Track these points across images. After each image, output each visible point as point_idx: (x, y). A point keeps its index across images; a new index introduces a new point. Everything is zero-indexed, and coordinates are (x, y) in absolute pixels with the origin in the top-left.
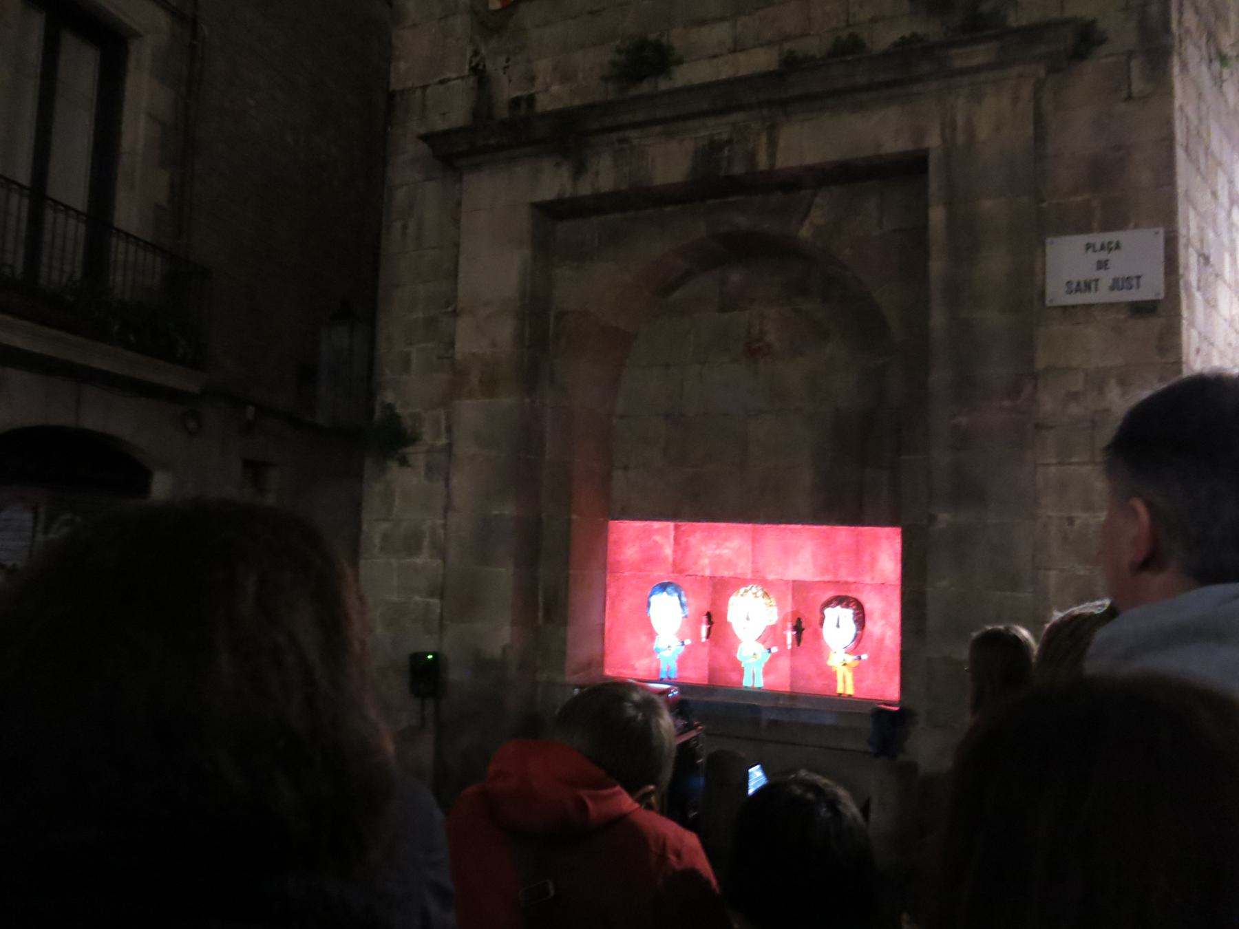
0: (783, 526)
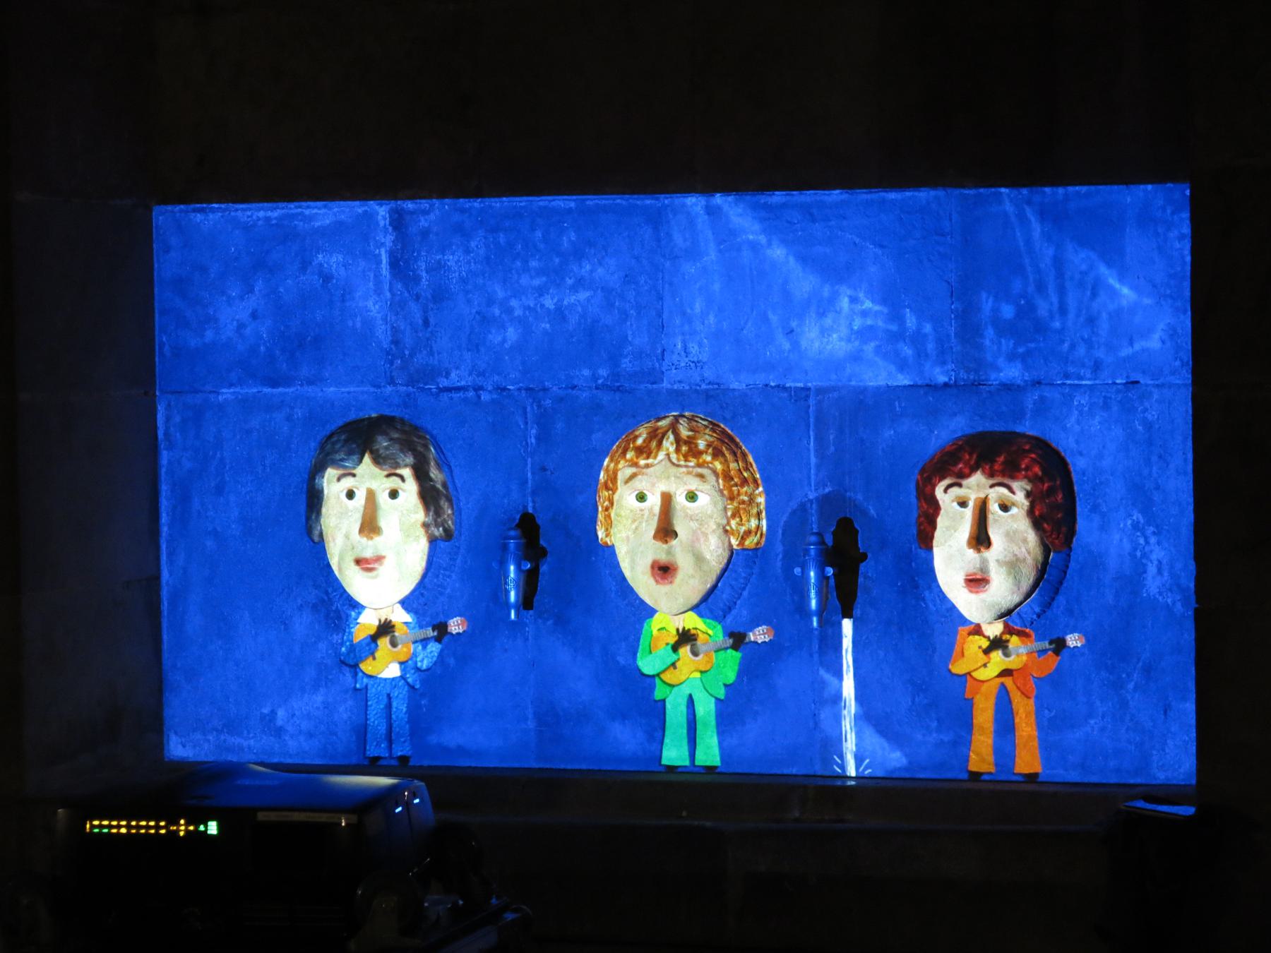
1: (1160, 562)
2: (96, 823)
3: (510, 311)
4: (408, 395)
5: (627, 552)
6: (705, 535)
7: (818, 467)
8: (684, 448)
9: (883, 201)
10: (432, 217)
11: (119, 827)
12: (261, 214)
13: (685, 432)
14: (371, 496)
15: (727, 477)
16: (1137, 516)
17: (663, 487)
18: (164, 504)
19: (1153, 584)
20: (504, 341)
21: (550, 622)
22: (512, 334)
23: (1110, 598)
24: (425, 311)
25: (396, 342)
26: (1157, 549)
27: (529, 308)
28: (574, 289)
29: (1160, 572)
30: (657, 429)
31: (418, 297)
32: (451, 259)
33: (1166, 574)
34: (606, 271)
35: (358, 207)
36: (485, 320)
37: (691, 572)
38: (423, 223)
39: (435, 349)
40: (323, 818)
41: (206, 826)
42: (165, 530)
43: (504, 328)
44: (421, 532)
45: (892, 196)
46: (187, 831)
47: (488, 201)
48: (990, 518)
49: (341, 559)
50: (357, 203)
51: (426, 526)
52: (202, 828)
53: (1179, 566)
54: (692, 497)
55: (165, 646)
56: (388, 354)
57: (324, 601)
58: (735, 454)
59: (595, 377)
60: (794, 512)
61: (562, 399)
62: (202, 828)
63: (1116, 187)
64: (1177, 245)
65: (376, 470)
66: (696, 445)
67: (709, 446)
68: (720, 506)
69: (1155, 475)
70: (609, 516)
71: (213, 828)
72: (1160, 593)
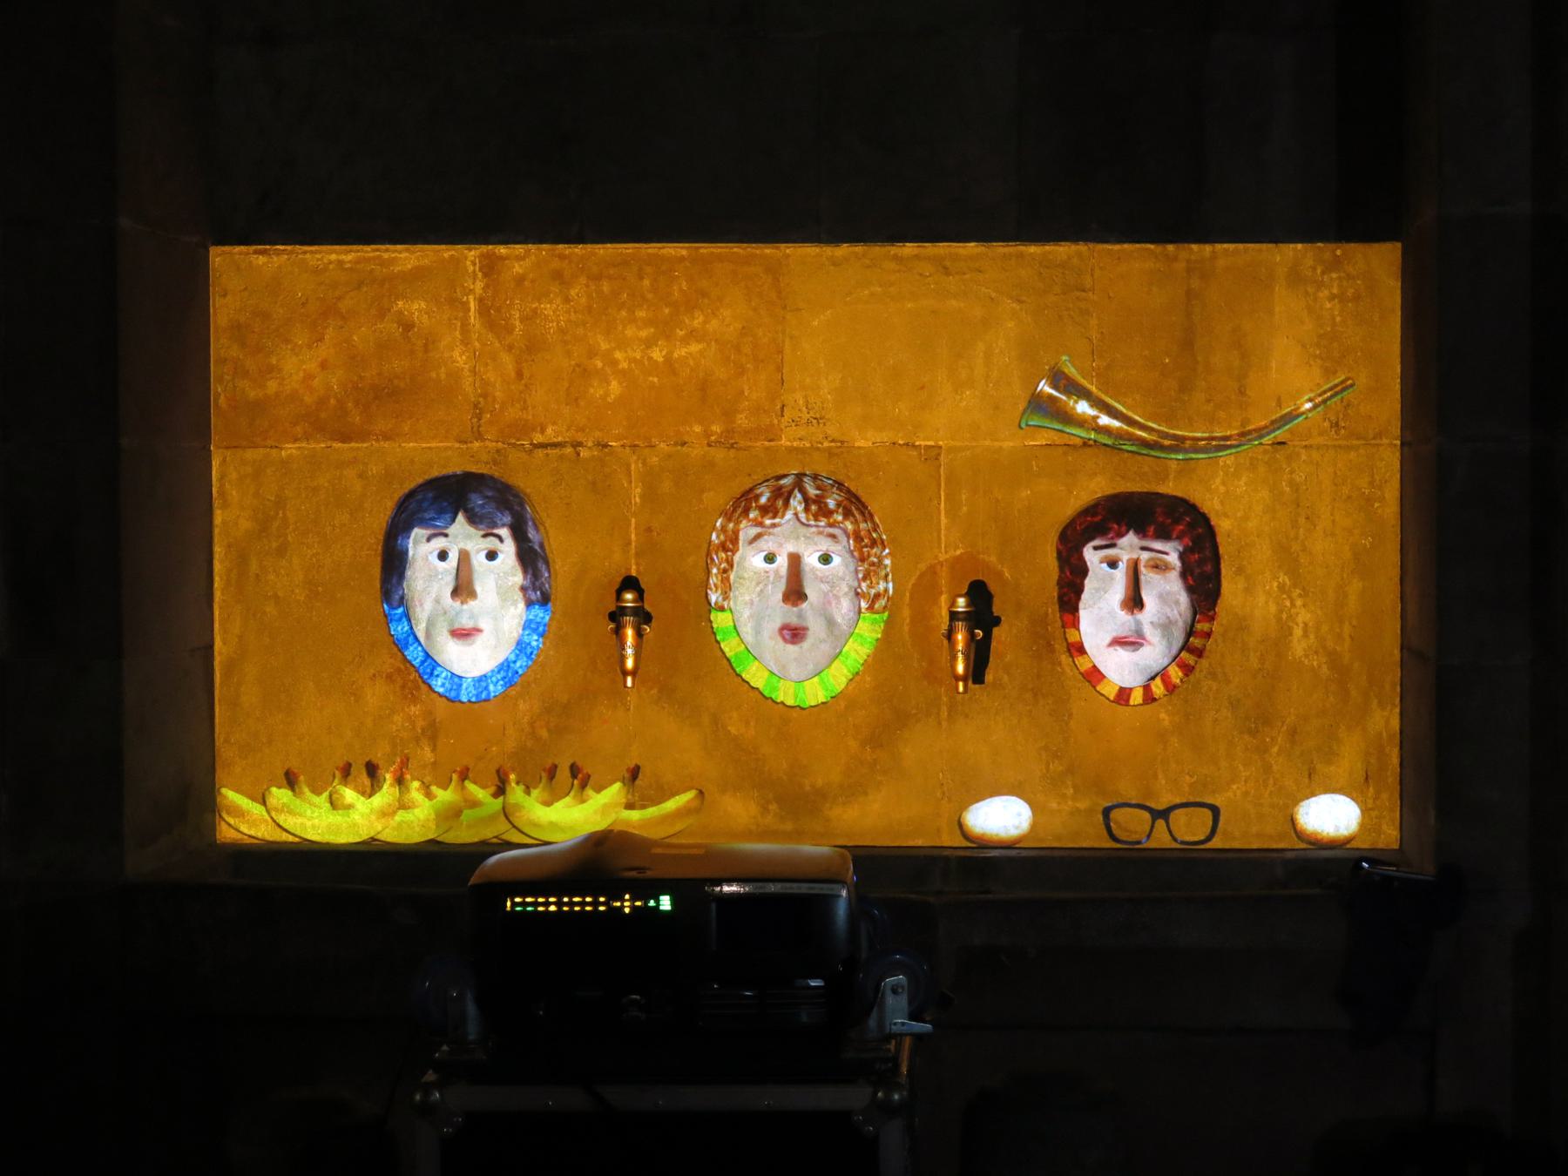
0: (909, 249)
1: (1306, 624)
2: (518, 900)
3: (614, 363)
4: (498, 451)
5: (751, 616)
6: (837, 597)
7: (947, 529)
8: (813, 507)
9: (1021, 256)
10: (527, 263)
11: (547, 904)
12: (333, 257)
13: (812, 492)
14: (464, 557)
15: (858, 537)
16: (1284, 578)
17: (791, 547)
18: (218, 567)
19: (1299, 646)
20: (607, 394)
21: (655, 691)
23: (1254, 662)
24: (518, 362)
25: (485, 396)
26: (1303, 611)
27: (635, 360)
28: (685, 341)
29: (1306, 634)
30: (781, 488)
31: (510, 348)
32: (547, 308)
33: (1312, 636)
34: (726, 320)
35: (447, 252)
36: (585, 373)
37: (823, 635)
38: (518, 269)
40: (804, 888)
41: (657, 901)
42: (218, 595)
43: (608, 384)
44: (519, 596)
45: (1033, 249)
46: (633, 908)
47: (589, 247)
48: (1142, 578)
49: (431, 624)
50: (443, 247)
51: (523, 589)
52: (652, 903)
53: (1325, 628)
54: (826, 559)
55: (217, 721)
56: (476, 406)
57: (399, 670)
58: (863, 514)
59: (707, 434)
60: (922, 575)
61: (670, 456)
62: (652, 903)
63: (1264, 246)
64: (1328, 305)
65: (472, 530)
66: (826, 504)
67: (839, 505)
68: (852, 568)
69: (1302, 537)
70: (728, 579)
71: (666, 903)
72: (1306, 656)
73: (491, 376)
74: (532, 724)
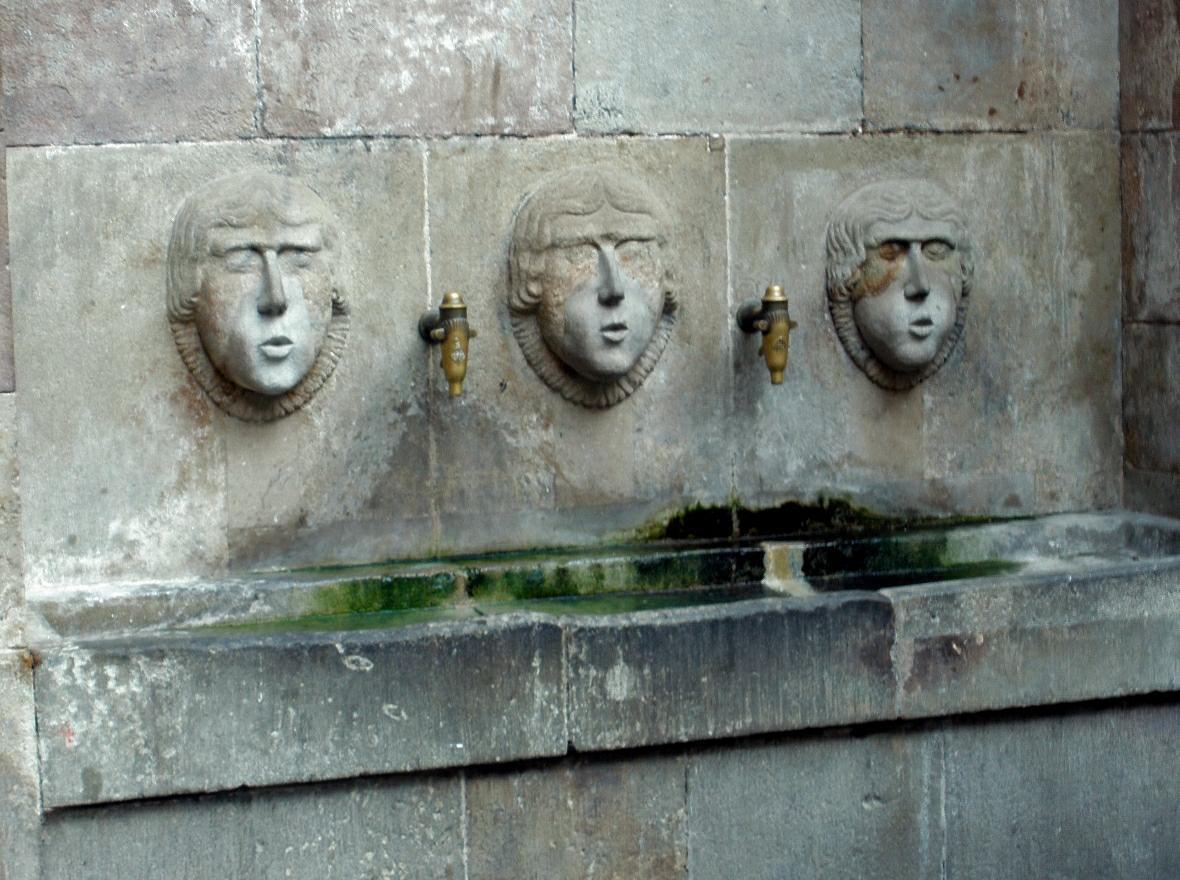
3: (404, 52)
20: (397, 86)
22: (406, 78)
24: (304, 49)
27: (426, 49)
31: (295, 35)
39: (316, 93)
43: (398, 71)
73: (276, 66)
74: (327, 440)
